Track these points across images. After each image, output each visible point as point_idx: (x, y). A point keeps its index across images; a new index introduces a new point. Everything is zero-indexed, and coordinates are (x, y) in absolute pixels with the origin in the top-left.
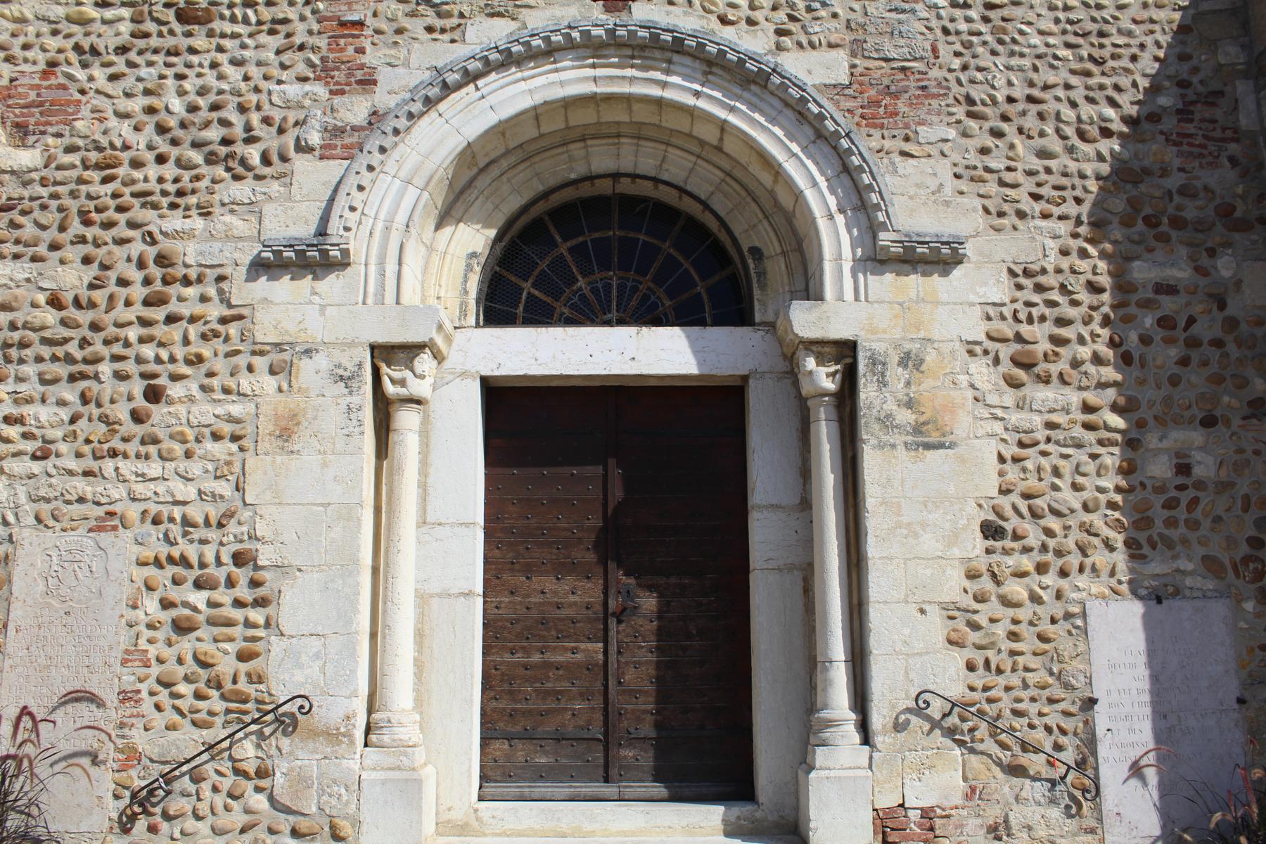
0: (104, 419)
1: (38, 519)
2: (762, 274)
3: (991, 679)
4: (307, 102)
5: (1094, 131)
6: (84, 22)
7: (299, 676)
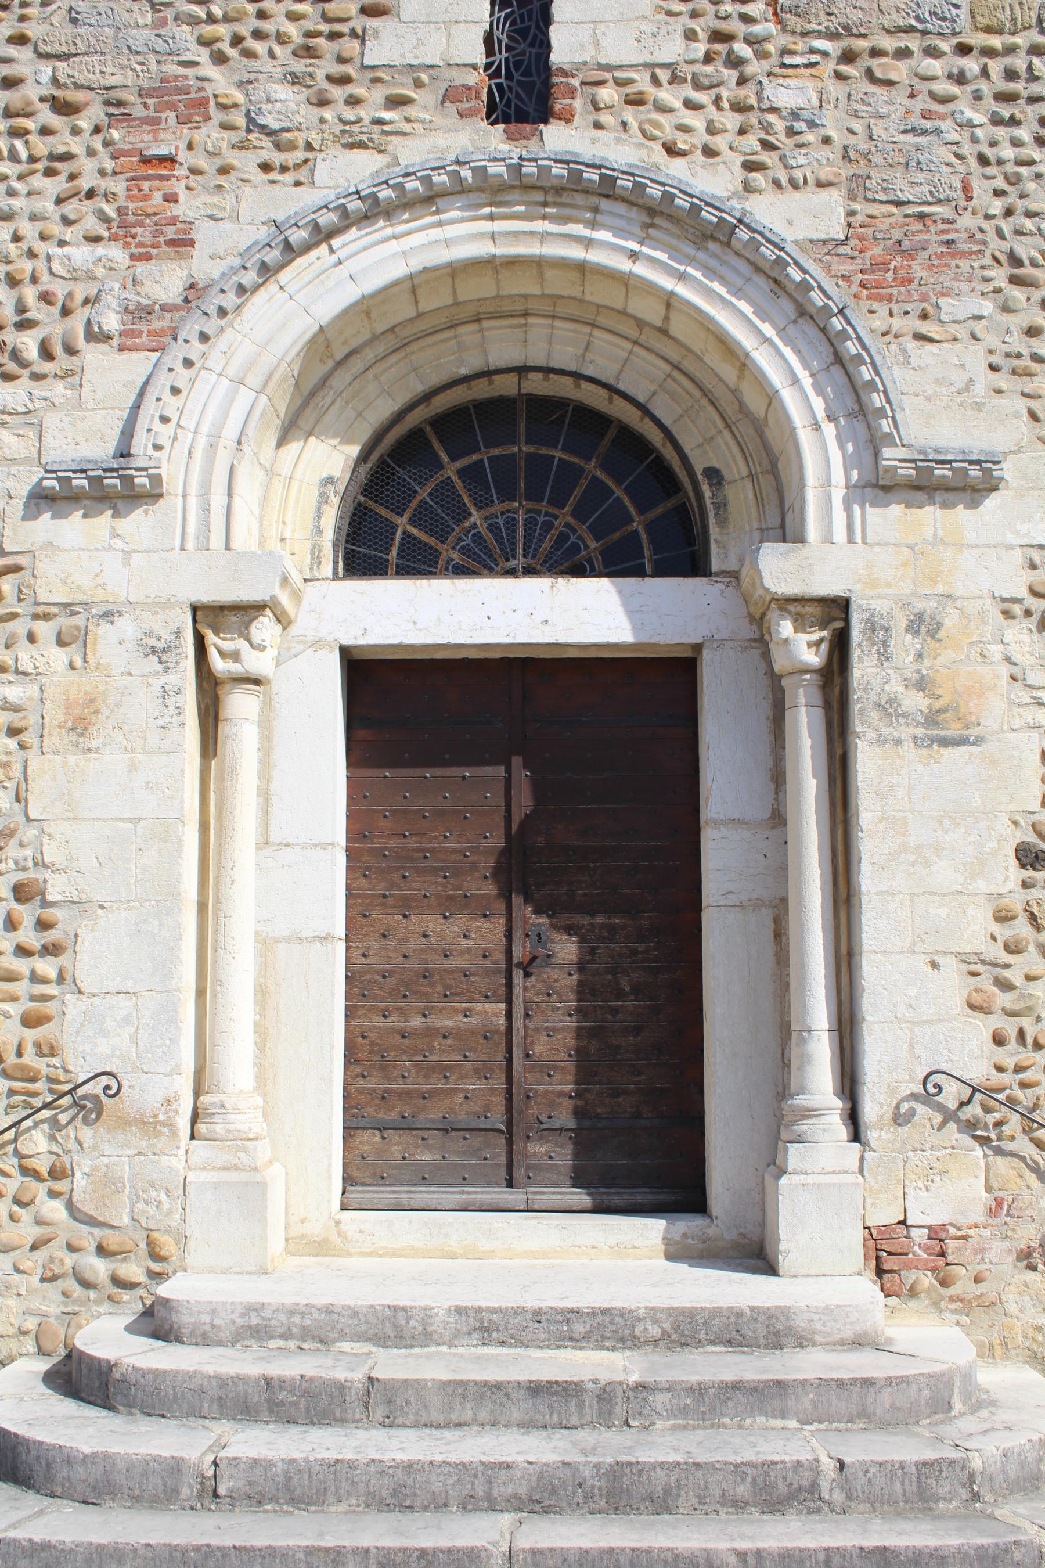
2: (721, 506)
3: (1026, 1056)
4: (100, 272)
7: (103, 1047)
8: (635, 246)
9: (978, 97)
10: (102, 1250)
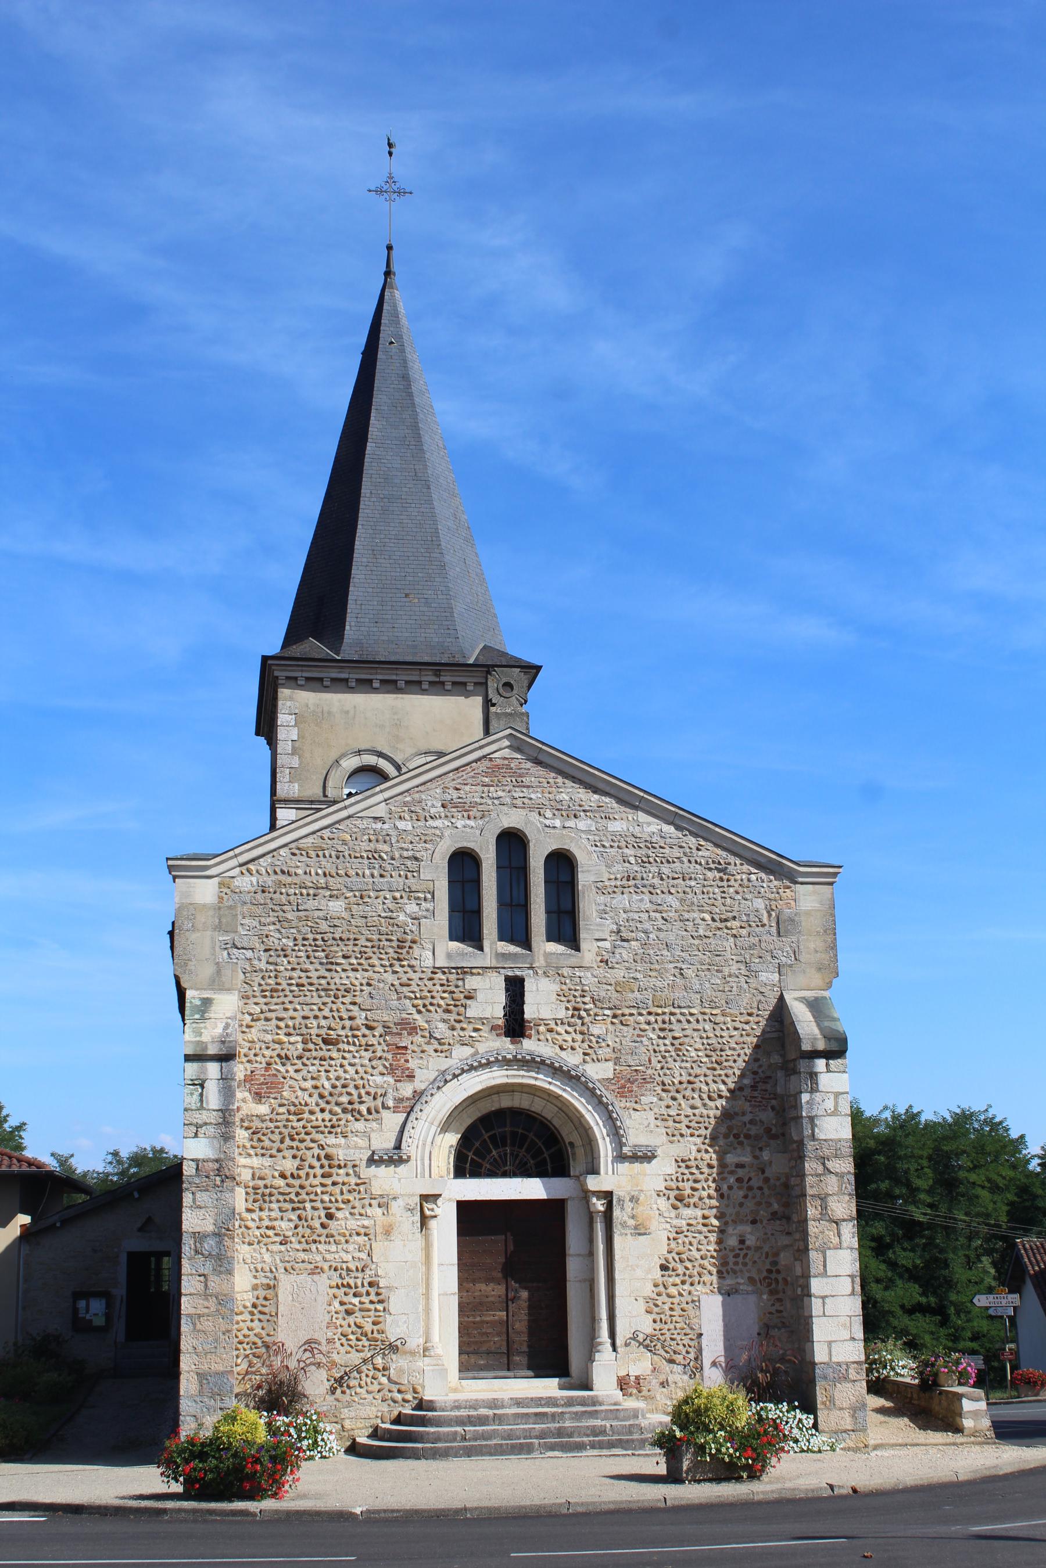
0: (310, 1227)
1: (286, 1269)
2: (574, 1154)
3: (662, 1326)
5: (715, 1096)
6: (280, 1043)
7: (398, 1330)
8: (550, 1080)
9: (654, 1029)
10: (399, 1391)
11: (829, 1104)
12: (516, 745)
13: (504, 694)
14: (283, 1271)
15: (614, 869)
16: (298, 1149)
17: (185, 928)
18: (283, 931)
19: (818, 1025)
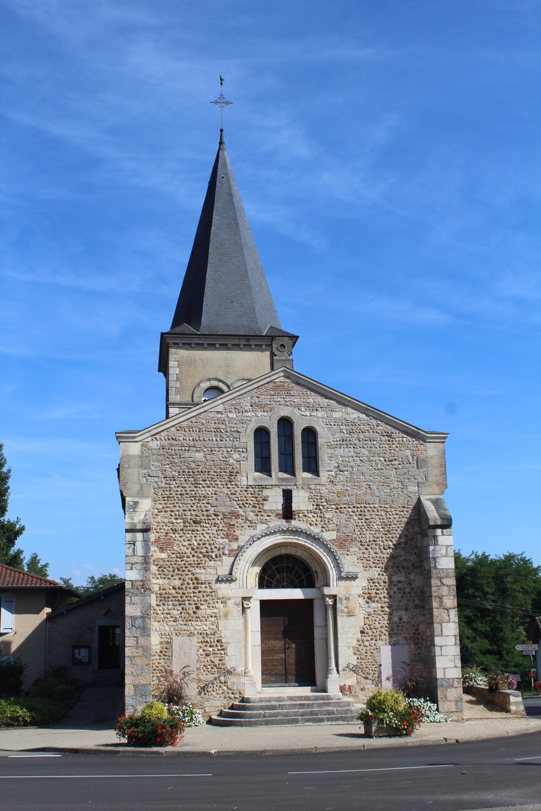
1: (176, 634)
2: (317, 577)
3: (362, 661)
5: (387, 547)
6: (172, 523)
7: (232, 664)
9: (356, 515)
10: (232, 693)
11: (443, 551)
12: (287, 375)
13: (281, 350)
14: (175, 634)
15: (336, 436)
16: (181, 575)
17: (125, 467)
18: (173, 468)
19: (438, 512)
